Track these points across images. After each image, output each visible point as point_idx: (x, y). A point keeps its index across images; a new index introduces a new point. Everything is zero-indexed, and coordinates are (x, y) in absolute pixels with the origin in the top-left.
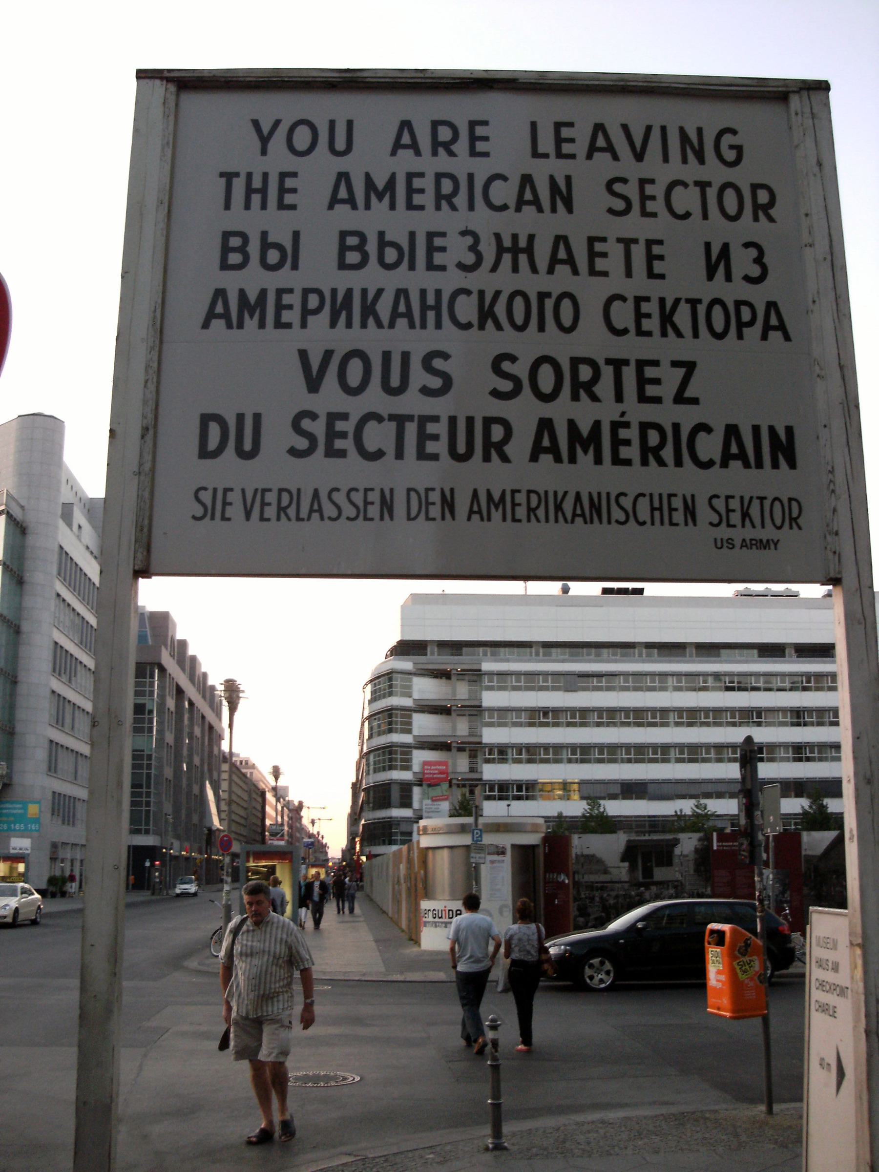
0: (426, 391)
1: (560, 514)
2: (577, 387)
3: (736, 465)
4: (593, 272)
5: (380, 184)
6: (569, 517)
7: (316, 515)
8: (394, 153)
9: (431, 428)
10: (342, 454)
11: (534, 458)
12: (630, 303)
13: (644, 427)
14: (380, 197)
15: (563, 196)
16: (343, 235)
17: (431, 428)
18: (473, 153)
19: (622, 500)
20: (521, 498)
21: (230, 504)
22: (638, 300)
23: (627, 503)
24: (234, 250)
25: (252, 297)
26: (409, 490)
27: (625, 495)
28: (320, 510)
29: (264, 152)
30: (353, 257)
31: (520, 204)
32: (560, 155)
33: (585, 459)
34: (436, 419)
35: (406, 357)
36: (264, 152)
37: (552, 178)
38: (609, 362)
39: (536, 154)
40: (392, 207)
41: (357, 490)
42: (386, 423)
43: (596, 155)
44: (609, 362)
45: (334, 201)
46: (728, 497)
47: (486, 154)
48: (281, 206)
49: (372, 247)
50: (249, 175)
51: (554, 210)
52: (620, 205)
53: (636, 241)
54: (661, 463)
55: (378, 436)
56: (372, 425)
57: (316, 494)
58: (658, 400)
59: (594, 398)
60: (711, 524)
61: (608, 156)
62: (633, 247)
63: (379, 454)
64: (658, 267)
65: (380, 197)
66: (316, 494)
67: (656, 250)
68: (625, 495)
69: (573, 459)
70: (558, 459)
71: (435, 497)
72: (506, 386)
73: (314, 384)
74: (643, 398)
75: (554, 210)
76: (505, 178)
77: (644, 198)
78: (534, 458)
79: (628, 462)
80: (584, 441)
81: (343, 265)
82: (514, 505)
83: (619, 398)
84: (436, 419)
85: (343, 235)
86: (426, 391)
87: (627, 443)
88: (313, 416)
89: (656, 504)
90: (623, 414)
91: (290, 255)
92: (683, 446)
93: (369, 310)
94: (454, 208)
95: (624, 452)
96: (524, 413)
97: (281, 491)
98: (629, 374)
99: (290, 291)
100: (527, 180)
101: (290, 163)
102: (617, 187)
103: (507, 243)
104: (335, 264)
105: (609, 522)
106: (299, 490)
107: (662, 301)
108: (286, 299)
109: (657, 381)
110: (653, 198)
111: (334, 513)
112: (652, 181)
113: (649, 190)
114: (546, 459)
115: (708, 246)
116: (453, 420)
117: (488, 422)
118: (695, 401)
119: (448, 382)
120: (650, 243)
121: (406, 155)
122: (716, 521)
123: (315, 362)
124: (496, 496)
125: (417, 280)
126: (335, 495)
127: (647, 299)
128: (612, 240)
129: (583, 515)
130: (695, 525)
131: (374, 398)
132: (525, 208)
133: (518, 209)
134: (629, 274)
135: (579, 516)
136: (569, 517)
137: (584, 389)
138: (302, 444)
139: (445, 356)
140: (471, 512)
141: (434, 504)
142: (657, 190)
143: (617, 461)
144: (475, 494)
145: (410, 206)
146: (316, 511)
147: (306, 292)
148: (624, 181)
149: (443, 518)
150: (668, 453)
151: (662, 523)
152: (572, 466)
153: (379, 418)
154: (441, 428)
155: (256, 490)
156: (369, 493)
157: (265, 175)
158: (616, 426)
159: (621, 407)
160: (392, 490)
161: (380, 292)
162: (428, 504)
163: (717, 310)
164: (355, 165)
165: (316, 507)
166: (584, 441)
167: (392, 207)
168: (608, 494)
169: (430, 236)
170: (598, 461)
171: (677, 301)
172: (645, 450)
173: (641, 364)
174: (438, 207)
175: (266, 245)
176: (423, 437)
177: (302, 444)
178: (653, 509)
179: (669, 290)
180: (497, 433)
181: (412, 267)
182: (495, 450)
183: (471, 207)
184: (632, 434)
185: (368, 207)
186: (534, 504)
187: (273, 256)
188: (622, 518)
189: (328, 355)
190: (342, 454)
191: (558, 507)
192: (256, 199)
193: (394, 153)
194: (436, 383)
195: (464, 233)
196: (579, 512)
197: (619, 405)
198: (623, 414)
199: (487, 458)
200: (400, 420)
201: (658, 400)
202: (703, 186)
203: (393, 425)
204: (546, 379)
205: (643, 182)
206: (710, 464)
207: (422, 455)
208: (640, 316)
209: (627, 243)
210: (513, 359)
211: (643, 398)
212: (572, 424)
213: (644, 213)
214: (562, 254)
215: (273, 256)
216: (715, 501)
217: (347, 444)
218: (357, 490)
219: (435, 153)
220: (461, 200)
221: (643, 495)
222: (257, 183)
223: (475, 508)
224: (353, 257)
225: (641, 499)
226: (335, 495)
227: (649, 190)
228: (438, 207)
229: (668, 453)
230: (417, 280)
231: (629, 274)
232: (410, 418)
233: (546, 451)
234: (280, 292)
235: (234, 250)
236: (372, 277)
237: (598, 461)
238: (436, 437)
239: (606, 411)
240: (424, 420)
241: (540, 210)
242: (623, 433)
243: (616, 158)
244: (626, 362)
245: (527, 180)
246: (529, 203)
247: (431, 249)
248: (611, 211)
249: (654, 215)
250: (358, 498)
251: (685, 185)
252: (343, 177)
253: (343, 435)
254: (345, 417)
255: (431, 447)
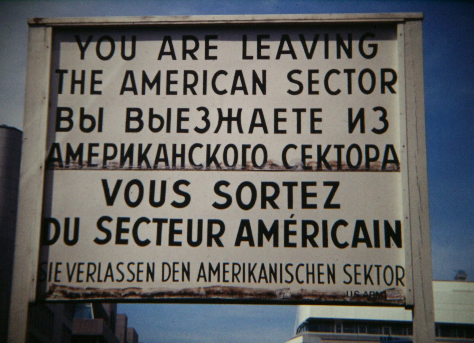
0: (175, 204)
1: (252, 277)
2: (264, 199)
3: (362, 246)
4: (277, 131)
5: (151, 79)
6: (257, 279)
7: (109, 279)
8: (160, 58)
9: (177, 227)
10: (125, 242)
11: (237, 244)
12: (299, 149)
13: (305, 223)
14: (151, 86)
15: (260, 83)
16: (129, 110)
17: (177, 227)
18: (207, 57)
19: (289, 268)
20: (229, 268)
21: (60, 272)
22: (304, 147)
23: (292, 270)
24: (65, 119)
25: (75, 149)
26: (164, 264)
27: (291, 265)
28: (112, 276)
29: (82, 57)
30: (134, 125)
31: (234, 88)
32: (260, 57)
33: (268, 244)
34: (180, 221)
35: (164, 183)
36: (82, 57)
37: (254, 73)
38: (285, 184)
39: (245, 57)
40: (158, 93)
41: (133, 264)
42: (151, 224)
43: (282, 56)
44: (285, 184)
45: (124, 89)
46: (356, 266)
47: (215, 58)
48: (93, 92)
49: (145, 118)
50: (74, 72)
51: (254, 92)
52: (296, 88)
53: (304, 110)
54: (315, 245)
55: (147, 231)
56: (143, 224)
57: (110, 266)
58: (314, 206)
59: (275, 206)
60: (345, 282)
61: (290, 56)
62: (302, 114)
63: (147, 242)
64: (318, 126)
65: (151, 86)
66: (110, 266)
67: (317, 115)
68: (291, 265)
69: (260, 244)
70: (252, 244)
71: (179, 268)
72: (223, 201)
73: (110, 201)
74: (305, 206)
75: (254, 92)
76: (225, 73)
77: (311, 82)
78: (237, 244)
79: (294, 245)
80: (268, 232)
81: (128, 130)
82: (225, 272)
83: (290, 206)
84: (180, 221)
85: (129, 110)
86: (175, 204)
87: (294, 233)
88: (109, 219)
89: (310, 270)
90: (292, 216)
91: (97, 123)
92: (329, 234)
93: (143, 157)
94: (194, 93)
95: (292, 239)
96: (232, 217)
97: (89, 264)
98: (297, 191)
99: (97, 145)
100: (239, 74)
101: (98, 64)
102: (295, 76)
103: (225, 114)
104: (124, 128)
105: (281, 282)
106: (100, 264)
107: (319, 147)
108: (95, 150)
109: (314, 195)
110: (317, 82)
111: (120, 277)
112: (317, 71)
113: (314, 77)
114: (245, 244)
115: (350, 111)
116: (190, 222)
117: (211, 223)
118: (337, 206)
119: (188, 197)
120: (313, 111)
121: (167, 58)
122: (348, 279)
123: (111, 188)
124: (214, 268)
125: (171, 139)
126: (120, 267)
127: (310, 147)
128: (289, 110)
129: (265, 277)
130: (334, 282)
131: (145, 209)
132: (237, 92)
133: (233, 93)
134: (299, 131)
135: (263, 278)
136: (257, 279)
137: (269, 201)
138: (103, 236)
139: (187, 183)
140: (199, 276)
141: (177, 271)
142: (320, 77)
143: (287, 244)
144: (202, 266)
145: (169, 92)
146: (109, 276)
147: (106, 146)
148: (299, 72)
149: (183, 280)
150: (319, 240)
151: (314, 282)
152: (260, 248)
153: (147, 221)
154: (183, 227)
155: (75, 264)
156: (140, 266)
157: (83, 72)
158: (287, 223)
159: (291, 212)
160: (154, 264)
161: (149, 146)
162: (174, 272)
163: (354, 151)
164: (137, 67)
165: (109, 274)
166: (268, 232)
167: (158, 93)
168: (281, 265)
169: (180, 111)
170: (276, 244)
171: (329, 147)
172: (305, 237)
173: (305, 185)
174: (185, 93)
175: (83, 117)
176: (173, 232)
177: (103, 236)
178: (308, 273)
179: (322, 140)
180: (216, 229)
181: (168, 130)
182: (215, 239)
183: (205, 92)
184: (297, 228)
185: (143, 93)
186: (236, 271)
187: (87, 123)
188: (289, 279)
189: (119, 183)
190: (125, 242)
191: (251, 273)
192: (78, 87)
193: (160, 58)
194: (181, 199)
195: (199, 109)
196: (263, 275)
197: (290, 210)
198: (292, 216)
199: (209, 244)
200: (160, 222)
201: (314, 206)
202: (349, 72)
203: (156, 224)
204: (246, 195)
205: (311, 72)
206: (345, 245)
207: (172, 243)
208: (304, 157)
209: (299, 111)
210: (226, 184)
211: (305, 206)
212: (261, 223)
213: (311, 92)
214: (258, 121)
215: (87, 123)
216: (347, 269)
217: (128, 236)
218: (133, 264)
219: (184, 58)
220: (199, 88)
221: (302, 265)
222: (78, 77)
223: (202, 274)
224: (134, 125)
225: (301, 267)
226: (120, 267)
227: (314, 77)
228: (185, 93)
229: (319, 240)
230: (171, 139)
231: (299, 131)
232: (165, 221)
233: (245, 239)
234: (91, 146)
235: (65, 119)
236: (145, 137)
237: (276, 244)
238: (180, 232)
239: (282, 214)
240: (173, 222)
241: (246, 93)
242: (292, 228)
243: (294, 57)
244: (296, 184)
245: (239, 74)
246: (239, 89)
247: (180, 119)
248: (290, 92)
249: (317, 93)
250: (134, 268)
251: (338, 72)
252: (130, 73)
253: (127, 231)
254: (127, 220)
255: (177, 238)
